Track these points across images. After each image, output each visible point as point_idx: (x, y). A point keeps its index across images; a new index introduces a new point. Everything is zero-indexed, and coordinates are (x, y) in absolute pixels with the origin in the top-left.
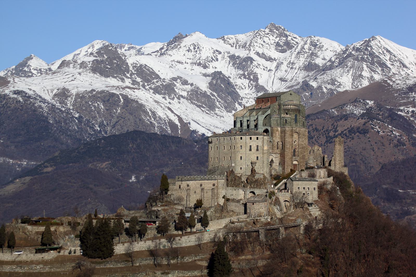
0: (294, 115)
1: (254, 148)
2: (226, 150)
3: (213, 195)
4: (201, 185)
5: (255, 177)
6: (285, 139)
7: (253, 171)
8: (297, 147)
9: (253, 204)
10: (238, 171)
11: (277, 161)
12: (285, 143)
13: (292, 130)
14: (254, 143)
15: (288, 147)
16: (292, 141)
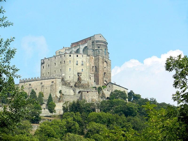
0: (104, 49)
1: (80, 63)
2: (57, 66)
3: (52, 90)
4: (42, 83)
5: (81, 83)
6: (98, 64)
7: (79, 79)
8: (106, 72)
9: (88, 92)
10: (68, 79)
11: (93, 79)
12: (98, 67)
13: (103, 59)
14: (80, 59)
15: (101, 69)
16: (103, 66)
